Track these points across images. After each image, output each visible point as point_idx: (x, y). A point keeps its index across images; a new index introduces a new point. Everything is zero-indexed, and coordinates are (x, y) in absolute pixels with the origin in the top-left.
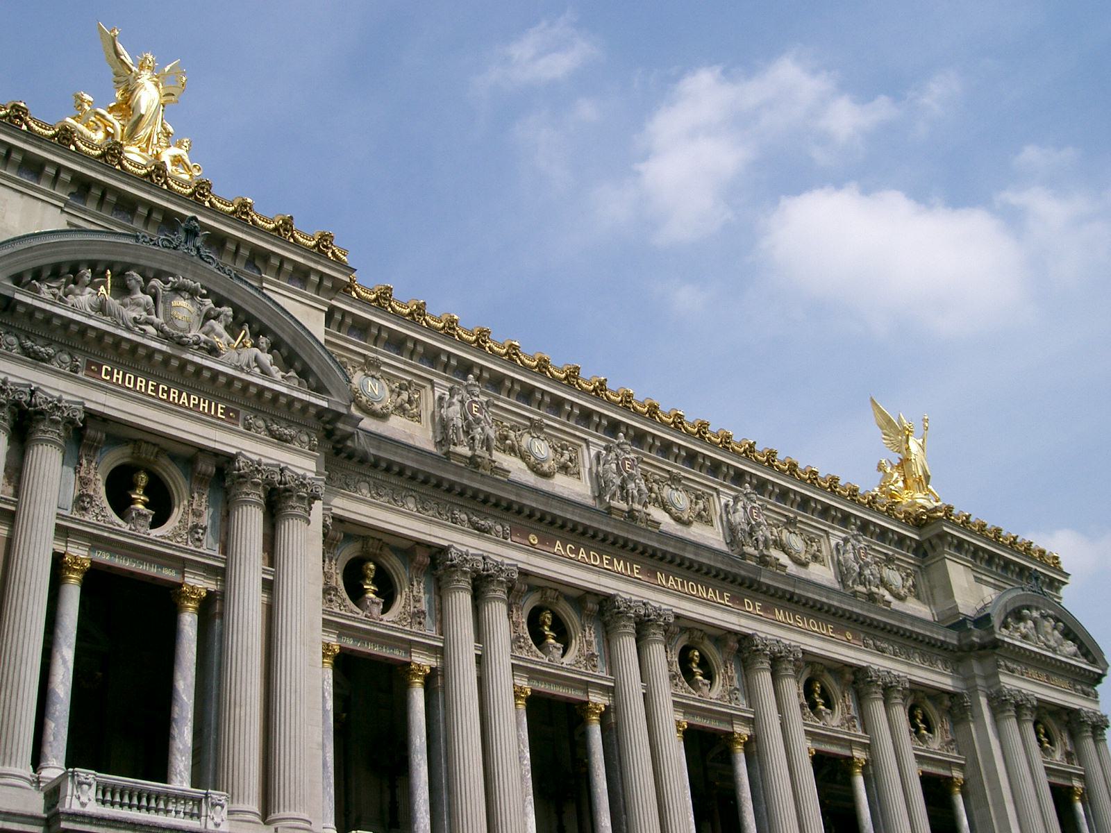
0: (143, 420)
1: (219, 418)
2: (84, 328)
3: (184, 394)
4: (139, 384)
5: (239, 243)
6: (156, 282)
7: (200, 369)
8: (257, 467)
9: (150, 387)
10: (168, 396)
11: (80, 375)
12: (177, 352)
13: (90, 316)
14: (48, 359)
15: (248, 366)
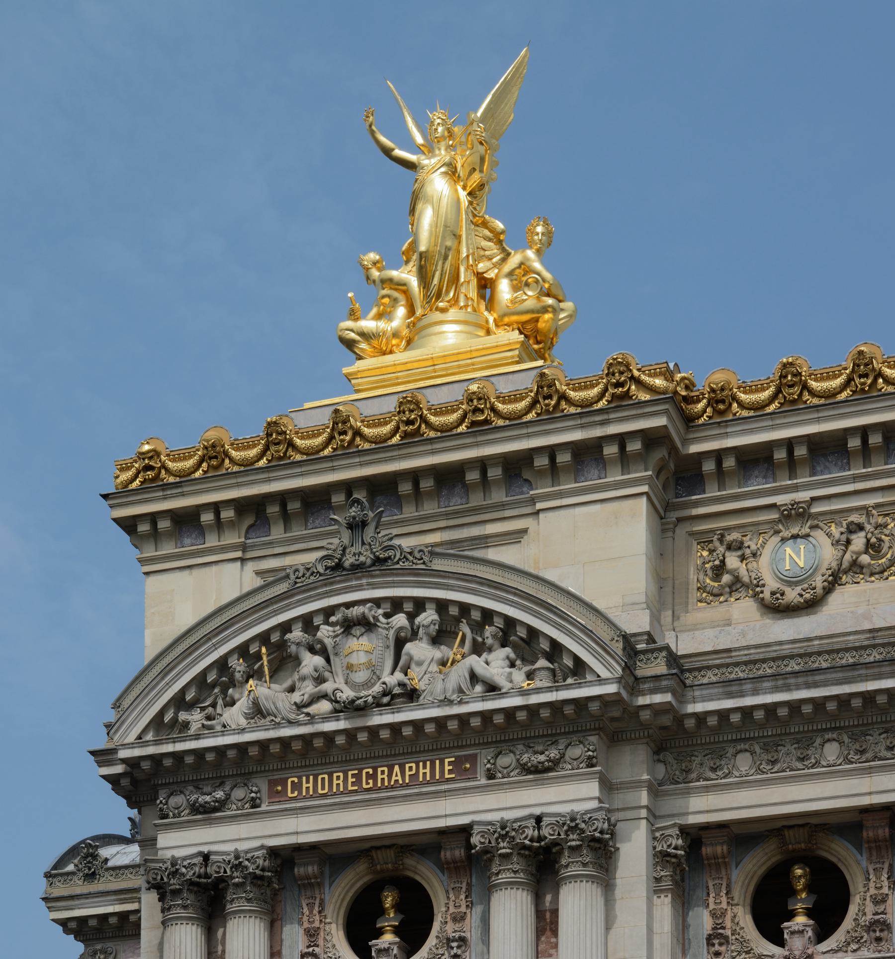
0: (346, 831)
1: (448, 780)
2: (242, 748)
3: (397, 768)
4: (335, 782)
5: (483, 464)
6: (325, 632)
7: (396, 728)
8: (504, 830)
9: (351, 780)
10: (375, 782)
11: (264, 807)
12: (359, 723)
13: (243, 731)
14: (221, 805)
15: (461, 691)
